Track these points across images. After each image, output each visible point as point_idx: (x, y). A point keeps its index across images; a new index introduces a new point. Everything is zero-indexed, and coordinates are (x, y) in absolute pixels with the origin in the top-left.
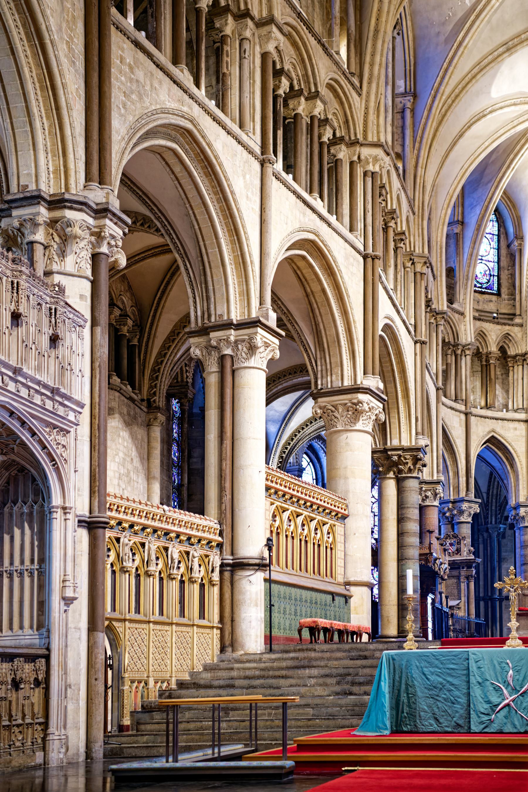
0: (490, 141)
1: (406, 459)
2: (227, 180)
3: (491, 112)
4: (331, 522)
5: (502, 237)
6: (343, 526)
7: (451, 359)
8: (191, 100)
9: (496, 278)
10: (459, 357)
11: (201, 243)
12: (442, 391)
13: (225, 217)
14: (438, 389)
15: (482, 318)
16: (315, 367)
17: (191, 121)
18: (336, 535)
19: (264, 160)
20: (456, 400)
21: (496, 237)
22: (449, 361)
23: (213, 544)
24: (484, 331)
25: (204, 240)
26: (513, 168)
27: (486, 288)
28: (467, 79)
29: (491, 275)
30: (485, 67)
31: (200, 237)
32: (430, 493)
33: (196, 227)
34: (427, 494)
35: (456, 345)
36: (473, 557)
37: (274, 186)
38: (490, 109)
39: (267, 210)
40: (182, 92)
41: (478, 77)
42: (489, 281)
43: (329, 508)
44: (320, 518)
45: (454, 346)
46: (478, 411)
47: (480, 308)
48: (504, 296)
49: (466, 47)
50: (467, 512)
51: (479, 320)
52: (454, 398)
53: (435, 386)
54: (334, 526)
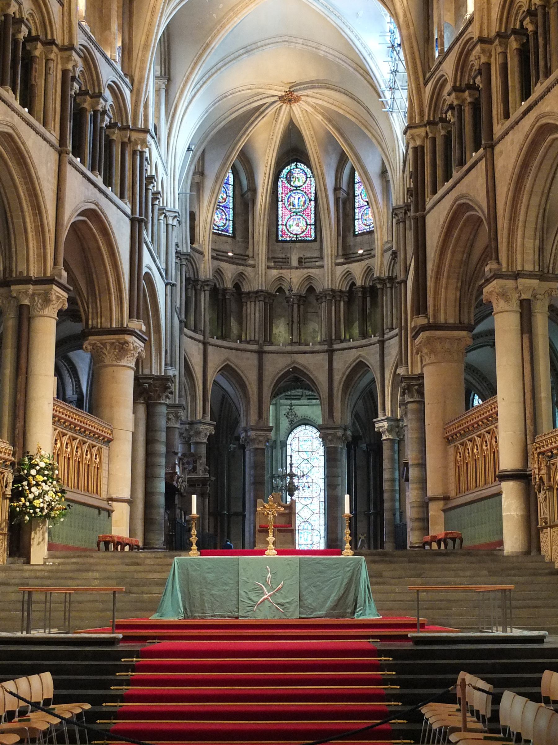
0: (229, 113)
1: (155, 387)
2: (34, 168)
3: (231, 94)
4: (99, 445)
5: (237, 187)
6: (108, 448)
7: (192, 293)
8: (13, 112)
9: (231, 222)
10: (198, 291)
11: (9, 214)
12: (184, 324)
13: (30, 196)
14: (181, 322)
15: (220, 257)
16: (86, 309)
17: (11, 127)
18: (102, 457)
19: (61, 151)
20: (195, 331)
21: (232, 187)
22: (189, 295)
23: (8, 463)
24: (221, 269)
25: (10, 212)
26: (248, 134)
27: (222, 231)
28: (213, 71)
29: (227, 220)
30: (228, 63)
31: (7, 209)
32: (172, 416)
33: (6, 202)
34: (170, 417)
35: (196, 281)
36: (208, 476)
37: (70, 172)
38: (230, 92)
39: (62, 190)
40: (7, 106)
41: (222, 69)
42: (225, 225)
43: (98, 434)
44: (91, 442)
45: (194, 281)
46: (212, 341)
47: (216, 248)
48: (237, 238)
49: (213, 48)
50: (203, 434)
51: (217, 259)
52: (193, 329)
53: (179, 319)
54: (101, 448)
